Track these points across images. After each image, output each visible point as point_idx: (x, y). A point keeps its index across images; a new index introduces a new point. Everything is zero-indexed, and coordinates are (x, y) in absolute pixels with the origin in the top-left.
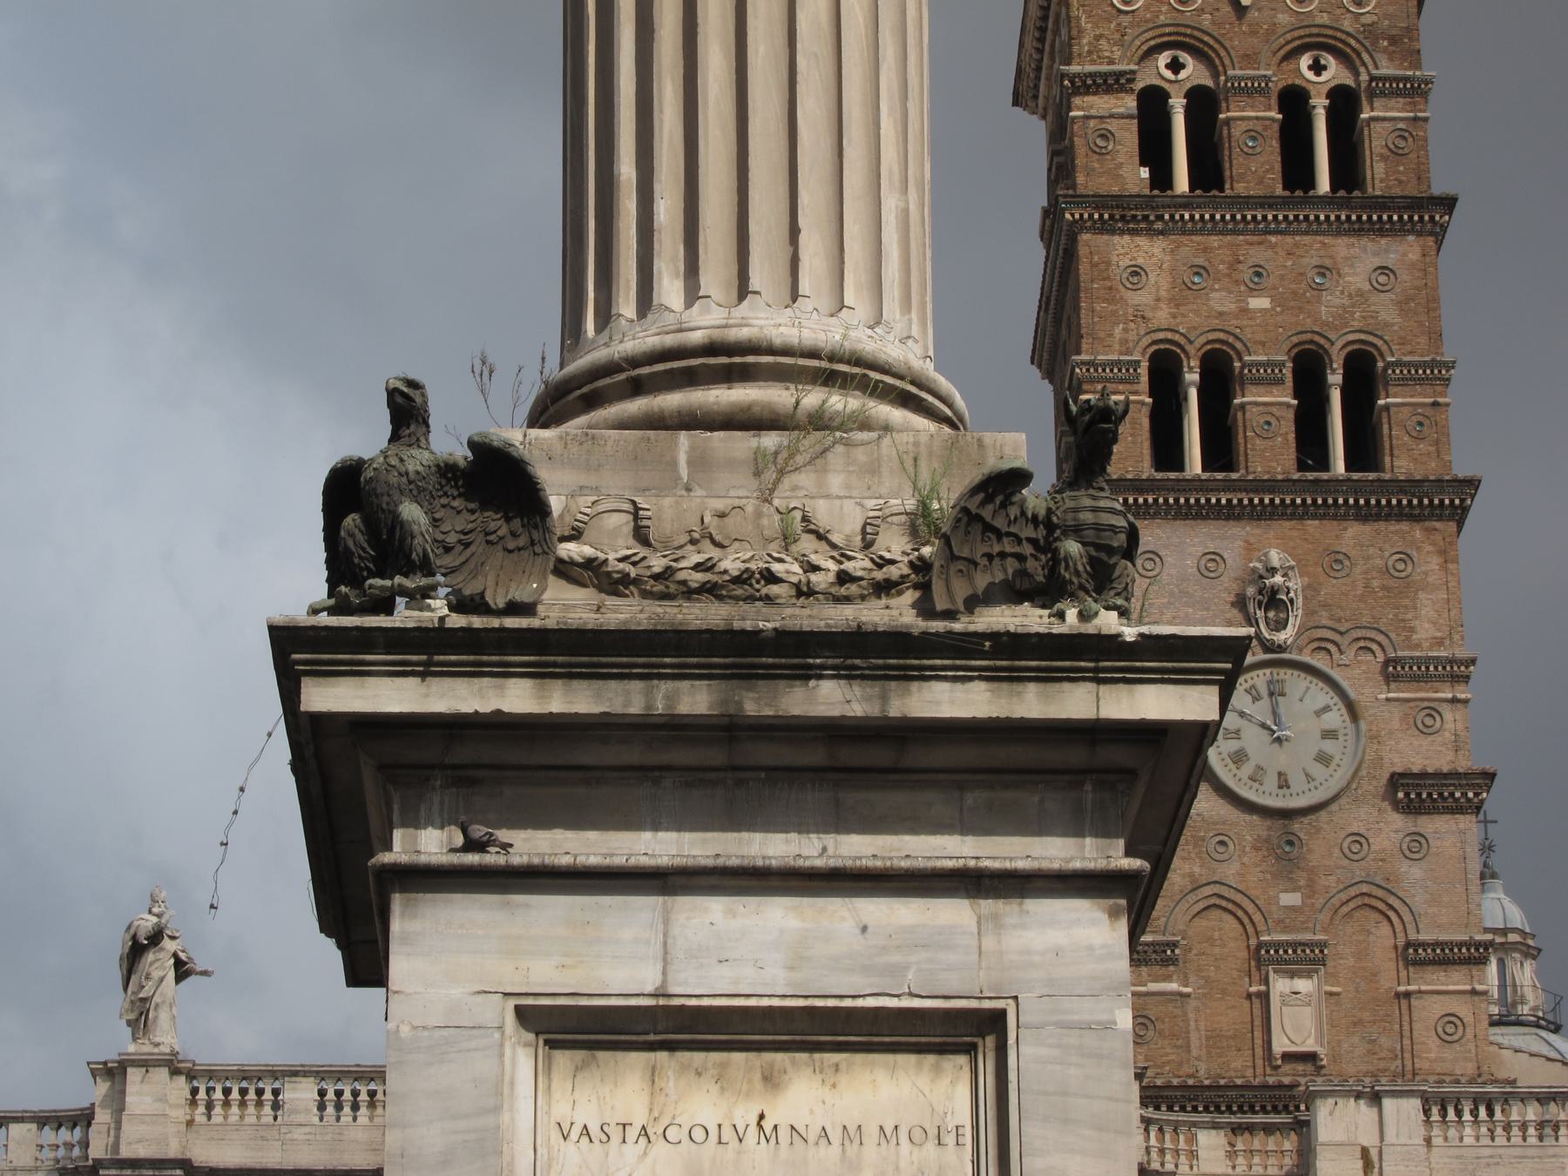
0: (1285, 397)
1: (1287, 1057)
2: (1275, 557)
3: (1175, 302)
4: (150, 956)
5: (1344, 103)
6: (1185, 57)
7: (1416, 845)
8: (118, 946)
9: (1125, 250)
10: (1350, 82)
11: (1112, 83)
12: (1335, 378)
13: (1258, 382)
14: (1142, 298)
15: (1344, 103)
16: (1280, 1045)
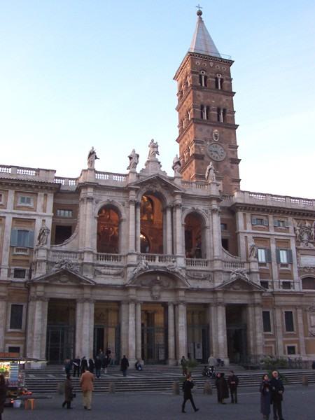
0: (216, 113)
2: (216, 131)
5: (222, 80)
7: (232, 167)
9: (198, 92)
11: (196, 73)
12: (222, 111)
15: (222, 80)
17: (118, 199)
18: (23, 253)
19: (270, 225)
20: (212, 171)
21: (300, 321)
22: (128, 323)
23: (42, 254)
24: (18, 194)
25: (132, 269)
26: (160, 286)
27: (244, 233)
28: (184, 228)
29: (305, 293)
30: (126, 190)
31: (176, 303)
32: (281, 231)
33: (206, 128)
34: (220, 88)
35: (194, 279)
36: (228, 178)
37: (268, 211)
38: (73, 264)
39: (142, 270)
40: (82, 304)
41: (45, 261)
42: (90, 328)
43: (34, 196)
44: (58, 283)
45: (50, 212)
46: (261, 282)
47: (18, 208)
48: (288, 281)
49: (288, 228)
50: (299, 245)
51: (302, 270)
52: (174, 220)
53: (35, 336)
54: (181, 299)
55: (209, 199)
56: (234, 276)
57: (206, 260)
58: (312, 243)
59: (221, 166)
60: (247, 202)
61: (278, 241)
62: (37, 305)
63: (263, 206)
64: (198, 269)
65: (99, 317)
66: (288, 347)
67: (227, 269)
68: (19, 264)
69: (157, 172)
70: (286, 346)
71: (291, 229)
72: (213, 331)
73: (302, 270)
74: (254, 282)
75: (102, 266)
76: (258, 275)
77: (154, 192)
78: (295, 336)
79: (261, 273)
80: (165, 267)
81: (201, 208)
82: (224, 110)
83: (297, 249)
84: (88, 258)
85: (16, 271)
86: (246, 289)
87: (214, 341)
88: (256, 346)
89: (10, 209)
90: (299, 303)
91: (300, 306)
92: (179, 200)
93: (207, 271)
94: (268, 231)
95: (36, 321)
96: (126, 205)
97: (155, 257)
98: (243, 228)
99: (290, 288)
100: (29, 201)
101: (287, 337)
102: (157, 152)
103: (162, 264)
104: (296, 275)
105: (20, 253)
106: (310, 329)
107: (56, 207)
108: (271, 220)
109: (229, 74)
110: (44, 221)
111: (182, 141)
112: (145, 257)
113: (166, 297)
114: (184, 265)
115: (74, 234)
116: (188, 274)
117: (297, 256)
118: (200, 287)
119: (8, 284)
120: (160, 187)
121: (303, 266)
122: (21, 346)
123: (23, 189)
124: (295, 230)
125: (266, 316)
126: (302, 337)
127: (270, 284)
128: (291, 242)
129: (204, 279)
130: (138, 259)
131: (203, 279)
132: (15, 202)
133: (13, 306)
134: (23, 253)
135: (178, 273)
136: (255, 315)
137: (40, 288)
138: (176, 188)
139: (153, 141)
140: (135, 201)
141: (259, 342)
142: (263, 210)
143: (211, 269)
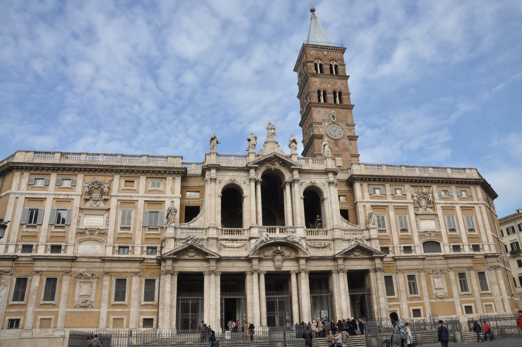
0: (332, 96)
1: (338, 166)
2: (333, 112)
3: (320, 85)
4: (214, 140)
5: (336, 66)
6: (319, 60)
7: (350, 144)
8: (210, 139)
9: (314, 79)
10: (337, 64)
12: (337, 94)
13: (329, 94)
14: (316, 84)
15: (336, 66)
16: (338, 165)
17: (240, 179)
18: (155, 232)
19: (387, 193)
20: (327, 147)
21: (424, 284)
22: (252, 293)
23: (170, 232)
24: (149, 180)
25: (253, 241)
26: (283, 255)
27: (362, 202)
28: (302, 201)
29: (427, 256)
30: (247, 169)
31: (297, 272)
32: (399, 198)
33: (323, 111)
34: (334, 73)
35: (314, 247)
36: (347, 154)
37: (384, 180)
38: (198, 239)
39: (262, 242)
40: (208, 276)
41: (173, 238)
42: (216, 298)
43: (164, 180)
44: (186, 257)
45: (178, 193)
46: (382, 248)
47: (150, 191)
49: (406, 195)
50: (419, 210)
51: (422, 234)
52: (293, 194)
53: (166, 307)
54: (302, 267)
55: (326, 172)
56: (353, 243)
57: (325, 229)
58: (431, 208)
59: (340, 143)
60: (363, 173)
61: (396, 208)
62: (167, 279)
63: (378, 176)
64: (318, 238)
65: (224, 288)
66: (414, 311)
67: (347, 237)
68: (150, 242)
69: (273, 151)
70: (412, 308)
71: (409, 196)
72: (336, 297)
73: (422, 234)
74: (373, 247)
75: (227, 240)
76: (378, 241)
77: (273, 169)
78: (420, 298)
79: (380, 239)
80: (286, 238)
81: (319, 181)
82: (340, 93)
83: (416, 215)
84: (213, 233)
85: (148, 248)
86: (366, 255)
87: (337, 307)
88: (380, 309)
89: (142, 192)
90: (422, 267)
91: (422, 270)
93: (327, 240)
94: (387, 199)
95: (166, 292)
96: (247, 183)
97: (275, 229)
98: (361, 198)
99: (411, 253)
100: (159, 185)
101: (412, 300)
104: (416, 239)
105: (151, 232)
106: (434, 292)
107: (184, 189)
108: (388, 188)
109: (342, 60)
110: (173, 202)
111: (304, 125)
112: (265, 230)
113: (288, 266)
114: (303, 236)
115: (201, 212)
116: (310, 244)
117: (417, 221)
118: (320, 255)
119: (142, 261)
120: (279, 165)
121: (423, 231)
122: (154, 317)
123: (154, 175)
124: (413, 197)
125: (388, 280)
126: (426, 301)
127: (390, 249)
128: (409, 208)
129: (325, 247)
130: (260, 232)
131: (323, 247)
132: (146, 187)
133: (145, 280)
134: (155, 232)
135: (297, 243)
136: (377, 280)
137: (169, 263)
138: (292, 165)
140: (255, 179)
141: (382, 306)
142: (380, 180)
143: (331, 238)
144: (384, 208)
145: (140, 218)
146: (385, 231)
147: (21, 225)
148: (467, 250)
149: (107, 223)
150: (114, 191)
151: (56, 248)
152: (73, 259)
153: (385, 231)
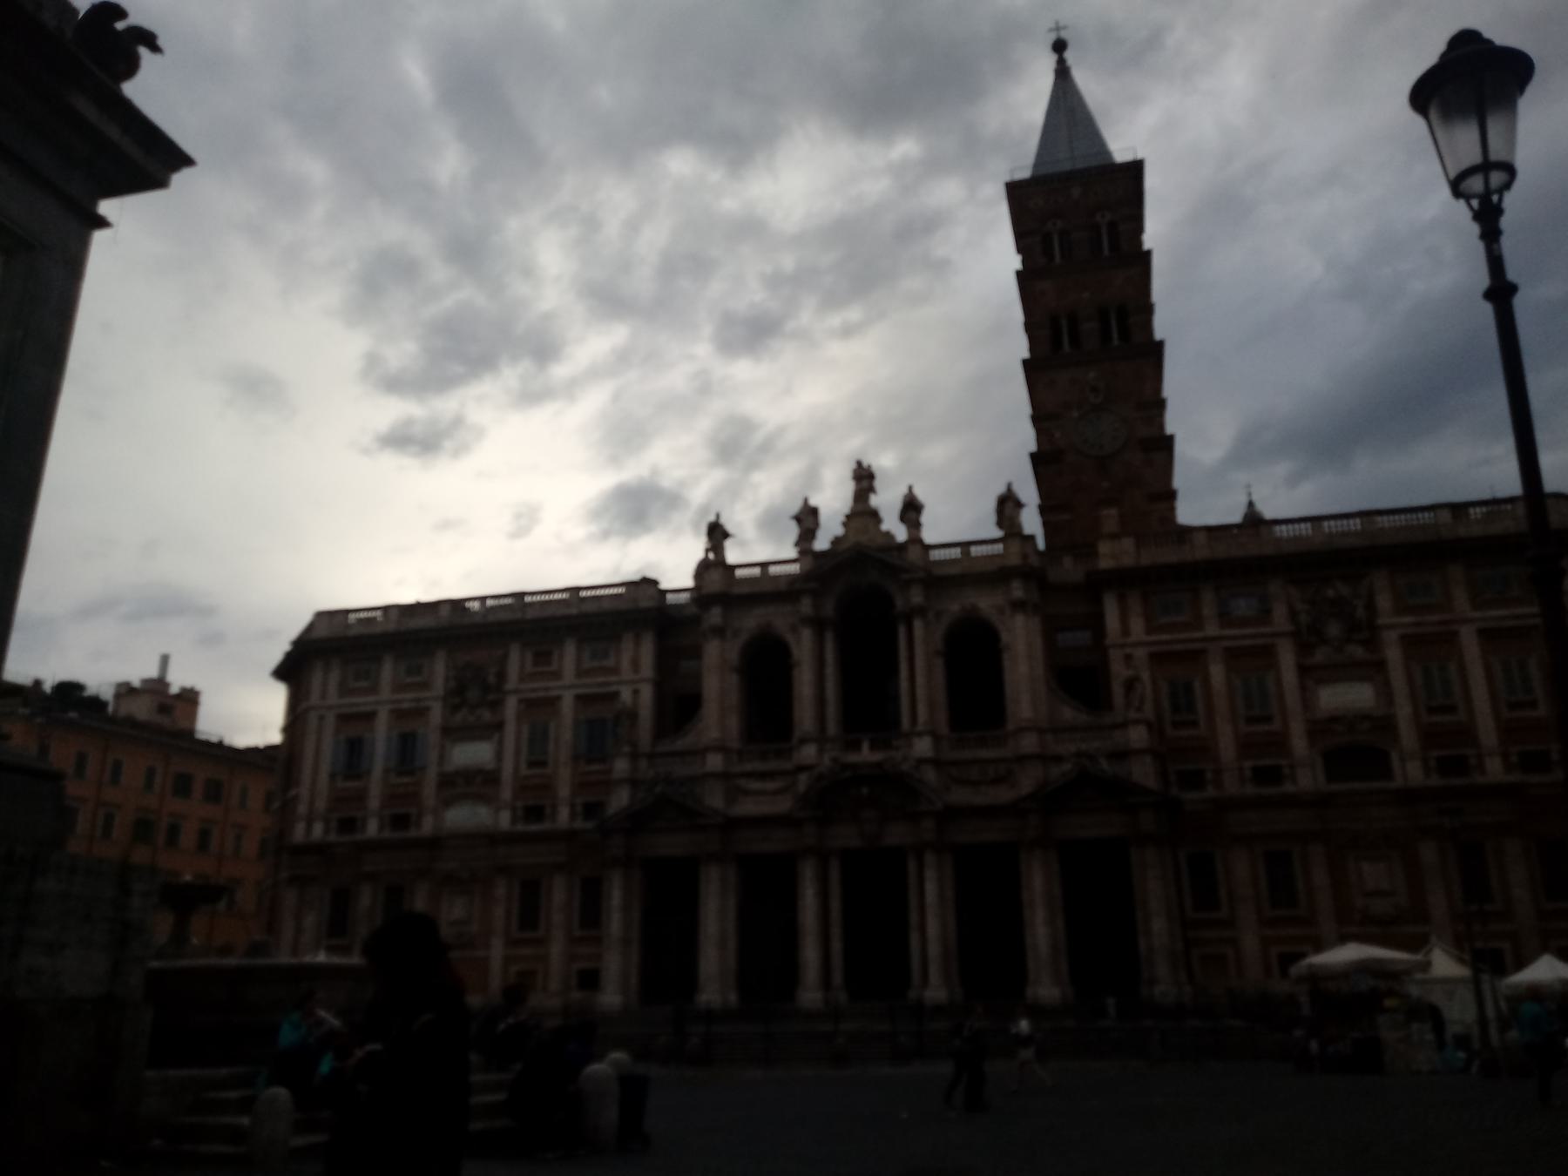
17: (779, 618)
20: (1009, 505)
23: (621, 766)
27: (1123, 646)
48: (1267, 762)
51: (1319, 728)
56: (1067, 767)
60: (1128, 561)
61: (1234, 656)
71: (1280, 614)
73: (1319, 728)
75: (749, 775)
76: (1148, 759)
80: (879, 765)
81: (986, 603)
83: (1303, 670)
84: (714, 762)
92: (917, 597)
102: (871, 489)
103: (877, 757)
117: (1303, 688)
119: (570, 836)
124: (1293, 614)
127: (1209, 775)
132: (579, 660)
139: (859, 464)
144: (1195, 656)
145: (567, 735)
146: (1194, 724)
147: (333, 776)
148: (1495, 769)
149: (499, 755)
150: (512, 682)
151: (400, 821)
152: (435, 843)
153: (1194, 724)
